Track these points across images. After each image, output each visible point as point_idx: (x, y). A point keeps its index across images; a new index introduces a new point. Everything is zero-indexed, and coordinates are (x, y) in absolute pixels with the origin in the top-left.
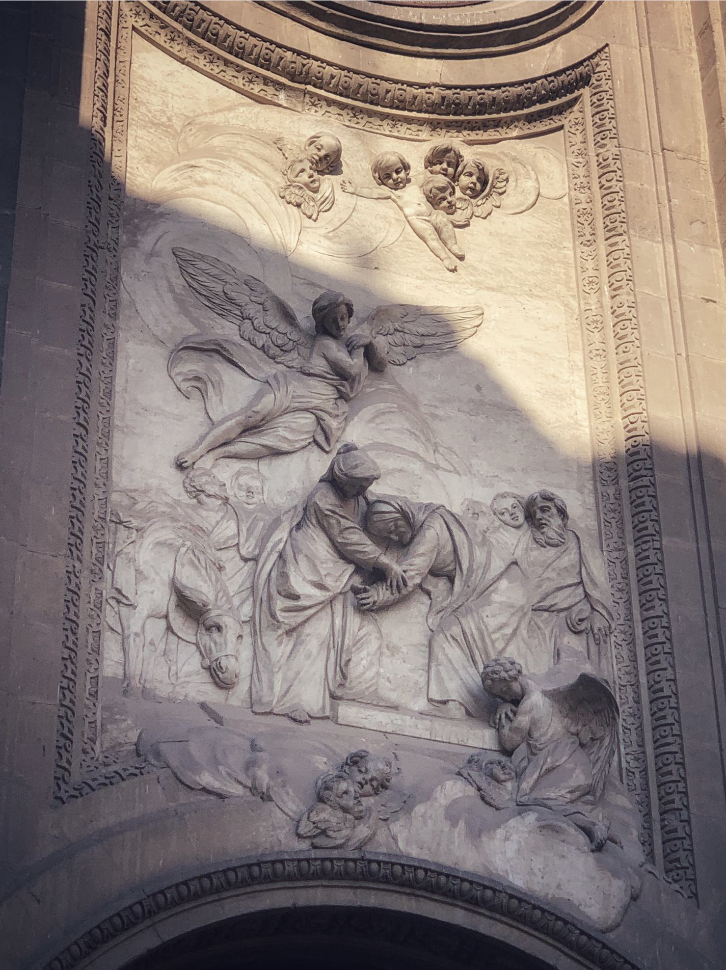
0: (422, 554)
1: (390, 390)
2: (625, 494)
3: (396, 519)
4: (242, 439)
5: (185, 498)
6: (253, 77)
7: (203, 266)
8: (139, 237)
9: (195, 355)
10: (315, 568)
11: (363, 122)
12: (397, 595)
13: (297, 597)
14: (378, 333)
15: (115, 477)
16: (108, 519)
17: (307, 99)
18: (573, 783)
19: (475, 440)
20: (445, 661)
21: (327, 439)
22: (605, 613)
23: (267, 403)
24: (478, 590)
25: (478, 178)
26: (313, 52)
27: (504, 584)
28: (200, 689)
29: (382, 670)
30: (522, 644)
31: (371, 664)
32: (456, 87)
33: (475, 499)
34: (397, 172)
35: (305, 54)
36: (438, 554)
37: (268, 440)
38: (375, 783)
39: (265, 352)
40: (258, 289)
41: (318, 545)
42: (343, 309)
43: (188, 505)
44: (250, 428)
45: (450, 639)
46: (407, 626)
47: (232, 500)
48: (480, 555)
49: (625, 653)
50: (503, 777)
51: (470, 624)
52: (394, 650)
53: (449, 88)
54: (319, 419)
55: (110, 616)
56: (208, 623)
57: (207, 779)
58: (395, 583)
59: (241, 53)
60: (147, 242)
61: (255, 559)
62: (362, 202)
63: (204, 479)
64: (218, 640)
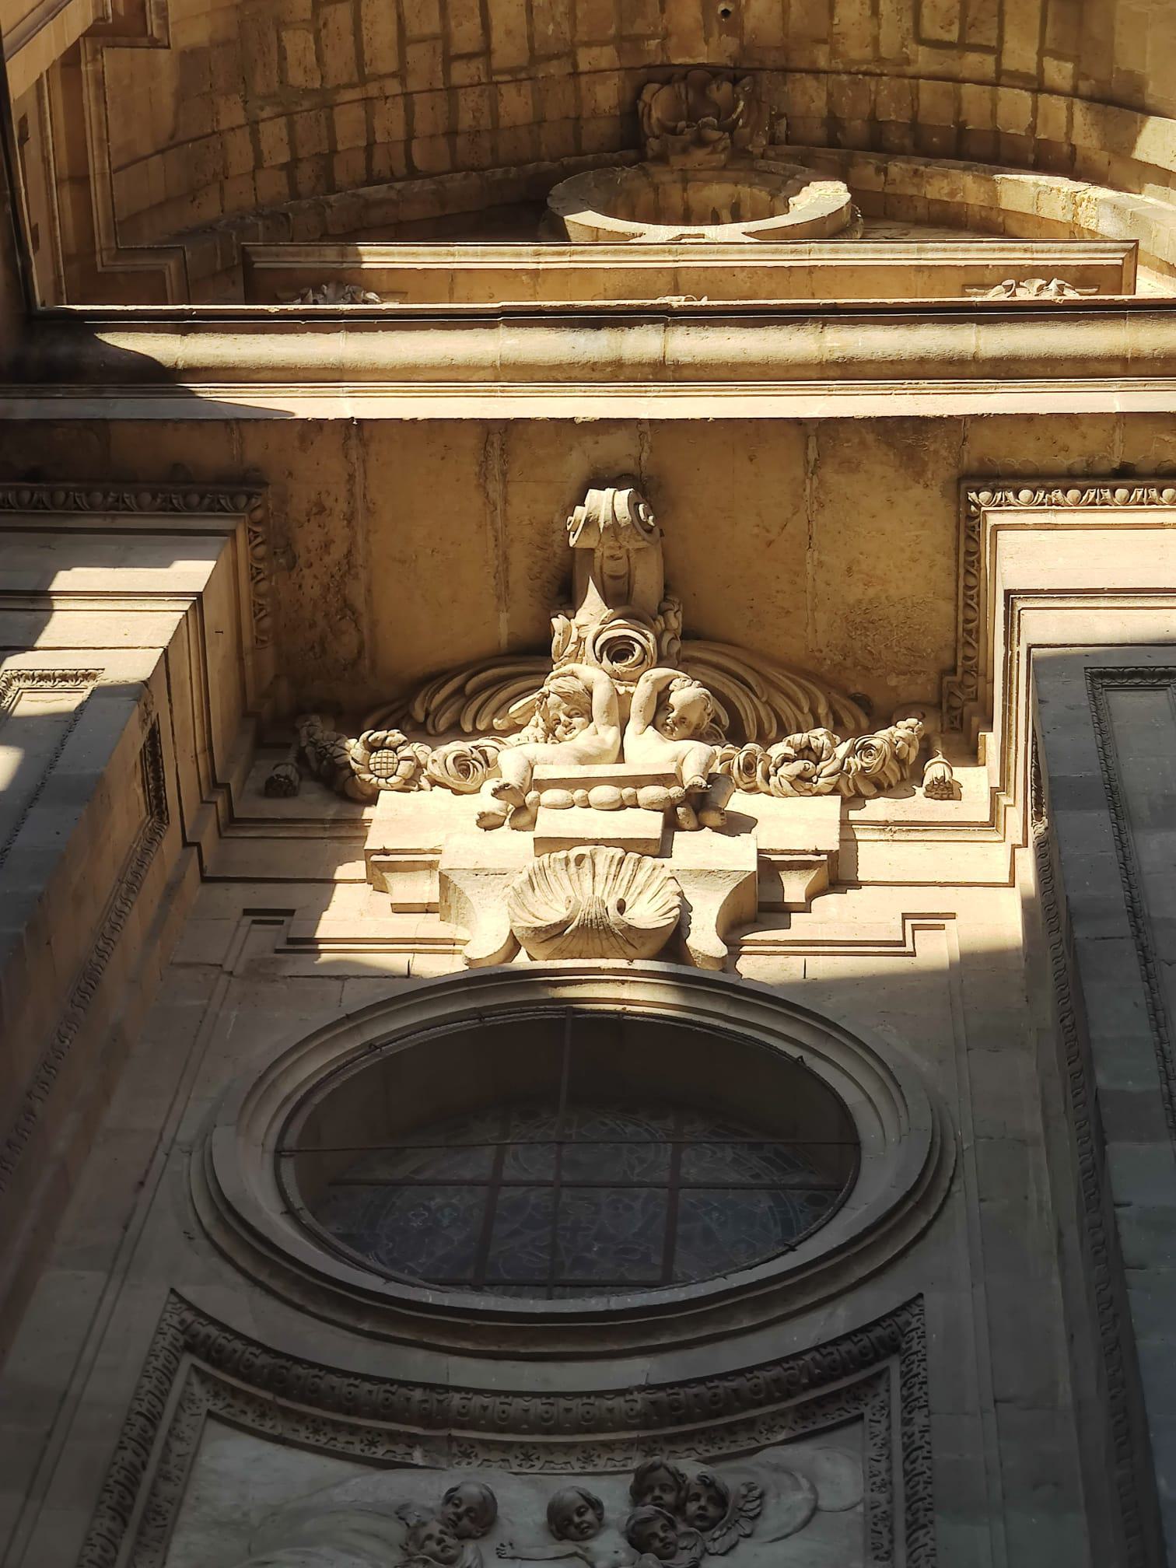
6: (373, 1438)
11: (538, 1464)
17: (455, 1450)
25: (710, 1499)
26: (452, 1382)
34: (580, 1514)
59: (351, 1406)
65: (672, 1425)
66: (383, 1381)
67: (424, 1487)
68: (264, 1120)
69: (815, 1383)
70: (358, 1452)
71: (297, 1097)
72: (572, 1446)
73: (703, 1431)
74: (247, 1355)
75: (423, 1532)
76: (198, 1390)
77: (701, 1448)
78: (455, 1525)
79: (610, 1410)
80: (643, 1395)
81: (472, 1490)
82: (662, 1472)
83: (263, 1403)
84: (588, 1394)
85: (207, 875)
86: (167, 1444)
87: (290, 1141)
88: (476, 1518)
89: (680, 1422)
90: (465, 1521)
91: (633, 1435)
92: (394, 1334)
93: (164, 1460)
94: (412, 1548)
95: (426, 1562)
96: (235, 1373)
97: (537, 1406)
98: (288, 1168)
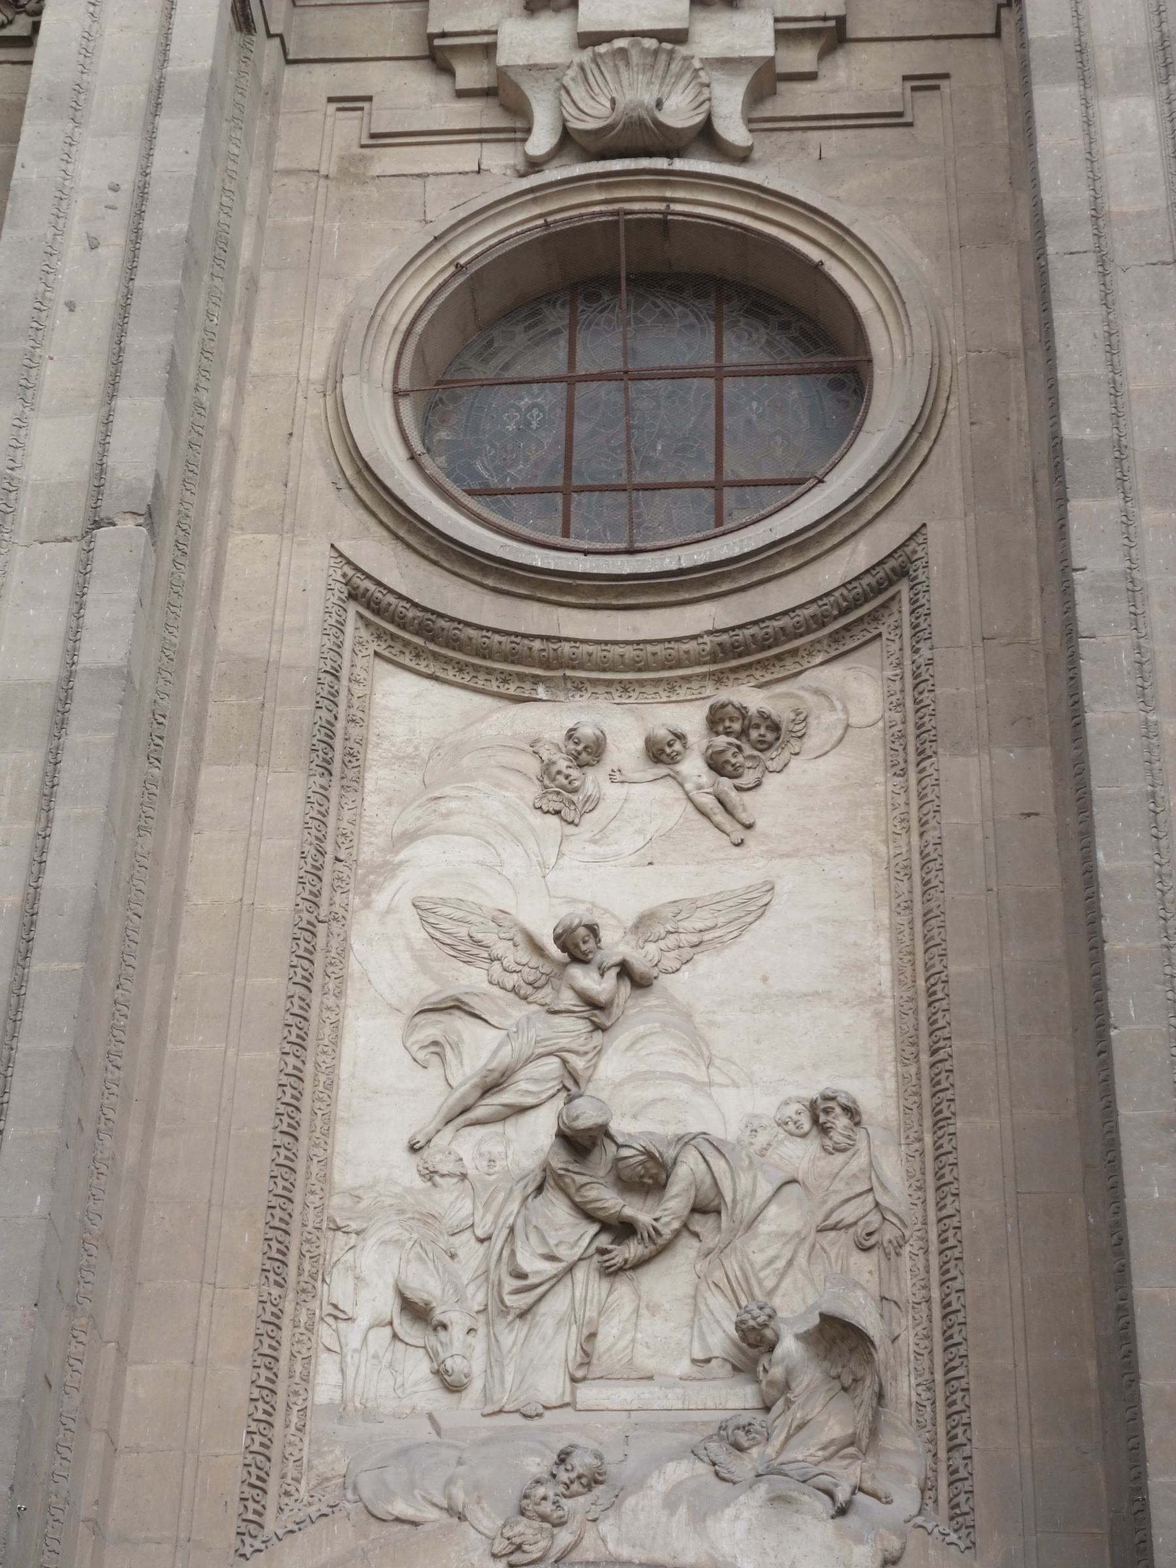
1: (657, 1006)
2: (926, 1071)
3: (642, 1163)
4: (483, 1102)
5: (419, 1183)
6: (506, 678)
7: (445, 911)
8: (374, 896)
10: (544, 1240)
11: (635, 695)
12: (652, 1247)
13: (522, 1276)
14: (646, 941)
15: (336, 1176)
16: (324, 1226)
17: (569, 685)
18: (825, 1438)
19: (758, 1042)
20: (708, 1315)
21: (576, 1083)
22: (895, 1220)
23: (506, 1056)
24: (745, 1223)
25: (767, 727)
26: (563, 634)
27: (773, 1210)
28: (429, 1396)
29: (639, 1336)
30: (800, 1276)
31: (624, 1332)
32: (733, 629)
33: (757, 1112)
34: (670, 745)
35: (554, 637)
36: (697, 1190)
37: (508, 1097)
38: (584, 1481)
39: (516, 994)
40: (506, 924)
42: (582, 931)
44: (491, 1086)
45: (712, 1287)
46: (670, 1280)
47: (471, 1172)
48: (744, 1181)
49: (921, 1263)
50: (746, 1444)
51: (733, 1265)
52: (654, 1309)
54: (565, 1062)
55: (325, 1334)
56: (434, 1322)
57: (400, 1508)
58: (645, 1235)
59: (485, 653)
60: (381, 900)
61: (489, 1238)
63: (439, 1157)
64: (443, 1340)
65: (734, 658)
66: (508, 633)
67: (551, 719)
68: (380, 357)
69: (843, 612)
70: (496, 689)
72: (660, 680)
73: (759, 662)
75: (554, 769)
76: (365, 634)
77: (758, 674)
78: (576, 758)
79: (687, 652)
80: (712, 638)
82: (730, 708)
84: (669, 641)
85: (290, 57)
87: (404, 383)
89: (740, 656)
90: (584, 755)
92: (513, 589)
94: (547, 782)
95: (558, 793)
96: (392, 621)
97: (629, 651)
98: (406, 406)
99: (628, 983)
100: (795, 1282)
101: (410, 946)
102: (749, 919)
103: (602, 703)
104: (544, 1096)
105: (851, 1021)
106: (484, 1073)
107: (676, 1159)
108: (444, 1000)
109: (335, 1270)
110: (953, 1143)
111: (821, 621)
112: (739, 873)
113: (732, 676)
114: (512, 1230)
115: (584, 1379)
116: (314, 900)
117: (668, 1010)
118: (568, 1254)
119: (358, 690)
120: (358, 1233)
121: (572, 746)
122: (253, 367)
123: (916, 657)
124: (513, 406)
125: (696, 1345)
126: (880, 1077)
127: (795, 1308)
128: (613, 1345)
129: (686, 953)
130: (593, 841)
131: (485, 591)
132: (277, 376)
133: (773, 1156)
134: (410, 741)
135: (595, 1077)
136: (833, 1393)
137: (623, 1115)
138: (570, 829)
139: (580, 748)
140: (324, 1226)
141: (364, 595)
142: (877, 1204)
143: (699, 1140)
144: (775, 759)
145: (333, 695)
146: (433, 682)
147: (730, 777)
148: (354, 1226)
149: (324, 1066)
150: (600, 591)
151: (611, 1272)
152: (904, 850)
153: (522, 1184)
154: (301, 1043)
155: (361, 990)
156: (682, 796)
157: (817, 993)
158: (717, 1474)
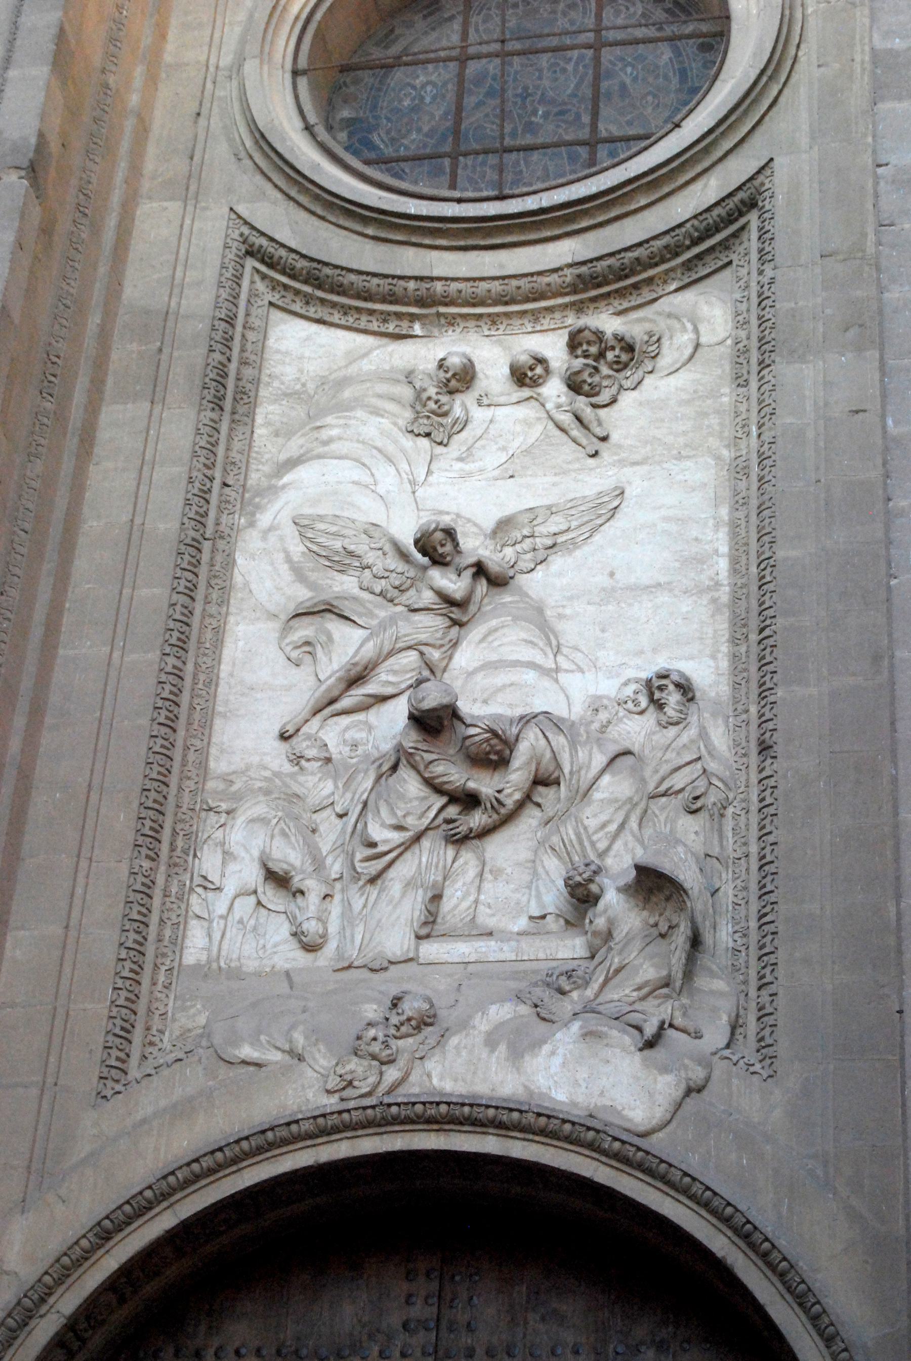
0: (518, 769)
1: (511, 602)
3: (487, 740)
5: (288, 768)
6: (385, 317)
7: (322, 526)
8: (258, 516)
9: (306, 620)
11: (502, 327)
12: (495, 816)
13: (373, 845)
14: (503, 546)
15: (212, 764)
16: (198, 807)
17: (443, 321)
18: (639, 980)
19: (603, 631)
20: (544, 876)
23: (369, 651)
24: (581, 791)
25: (622, 349)
26: (436, 273)
27: (606, 779)
28: (290, 956)
30: (630, 838)
32: (591, 261)
33: (599, 693)
34: (531, 369)
35: (428, 278)
36: (538, 764)
37: (371, 688)
38: (413, 1023)
40: (376, 535)
41: (410, 785)
42: (439, 535)
43: (287, 775)
44: (355, 679)
48: (582, 754)
50: (567, 988)
51: (569, 831)
52: (497, 873)
53: (583, 263)
54: (422, 654)
56: (294, 889)
57: (247, 1052)
58: (489, 805)
60: (264, 519)
62: (501, 412)
63: (304, 744)
66: (386, 276)
67: (427, 352)
68: (281, 42)
69: (695, 242)
70: (376, 329)
71: (304, 16)
72: (524, 312)
73: (617, 291)
74: (290, 261)
75: (424, 396)
76: (261, 286)
77: (616, 303)
78: (446, 385)
79: (549, 285)
80: (571, 270)
81: (455, 361)
82: (587, 332)
83: (306, 295)
84: (532, 275)
86: (243, 336)
87: (303, 63)
88: (460, 379)
89: (599, 286)
90: (453, 383)
91: (567, 299)
93: (243, 350)
94: (419, 408)
95: (428, 417)
96: (283, 272)
97: (496, 287)
98: (303, 82)
99: (484, 582)
100: (626, 844)
101: (288, 559)
102: (599, 521)
103: (473, 336)
104: (403, 686)
105: (690, 608)
106: (348, 667)
107: (518, 736)
108: (315, 605)
109: (205, 847)
110: (774, 711)
111: (674, 251)
112: (594, 480)
113: (592, 306)
114: (365, 804)
115: (428, 936)
116: (200, 520)
117: (521, 605)
118: (415, 823)
119: (251, 336)
120: (228, 813)
121: (442, 374)
122: (168, 58)
123: (761, 278)
124: (409, 84)
125: (533, 903)
126: (713, 657)
127: (620, 863)
128: (456, 906)
129: (541, 555)
130: (460, 459)
131: (367, 240)
132: (188, 65)
133: (613, 732)
134: (298, 379)
135: (451, 666)
136: (648, 940)
137: (475, 700)
138: (439, 450)
139: (449, 375)
140: (198, 807)
141: (259, 251)
142: (705, 771)
143: (540, 717)
144: (629, 377)
145: (227, 340)
146: (321, 326)
147: (587, 396)
148: (224, 806)
149: (204, 666)
150: (469, 232)
151: (459, 840)
152: (744, 452)
153: (377, 764)
154: (182, 645)
155: (242, 599)
156: (546, 415)
157: (659, 585)
158: (538, 1015)
